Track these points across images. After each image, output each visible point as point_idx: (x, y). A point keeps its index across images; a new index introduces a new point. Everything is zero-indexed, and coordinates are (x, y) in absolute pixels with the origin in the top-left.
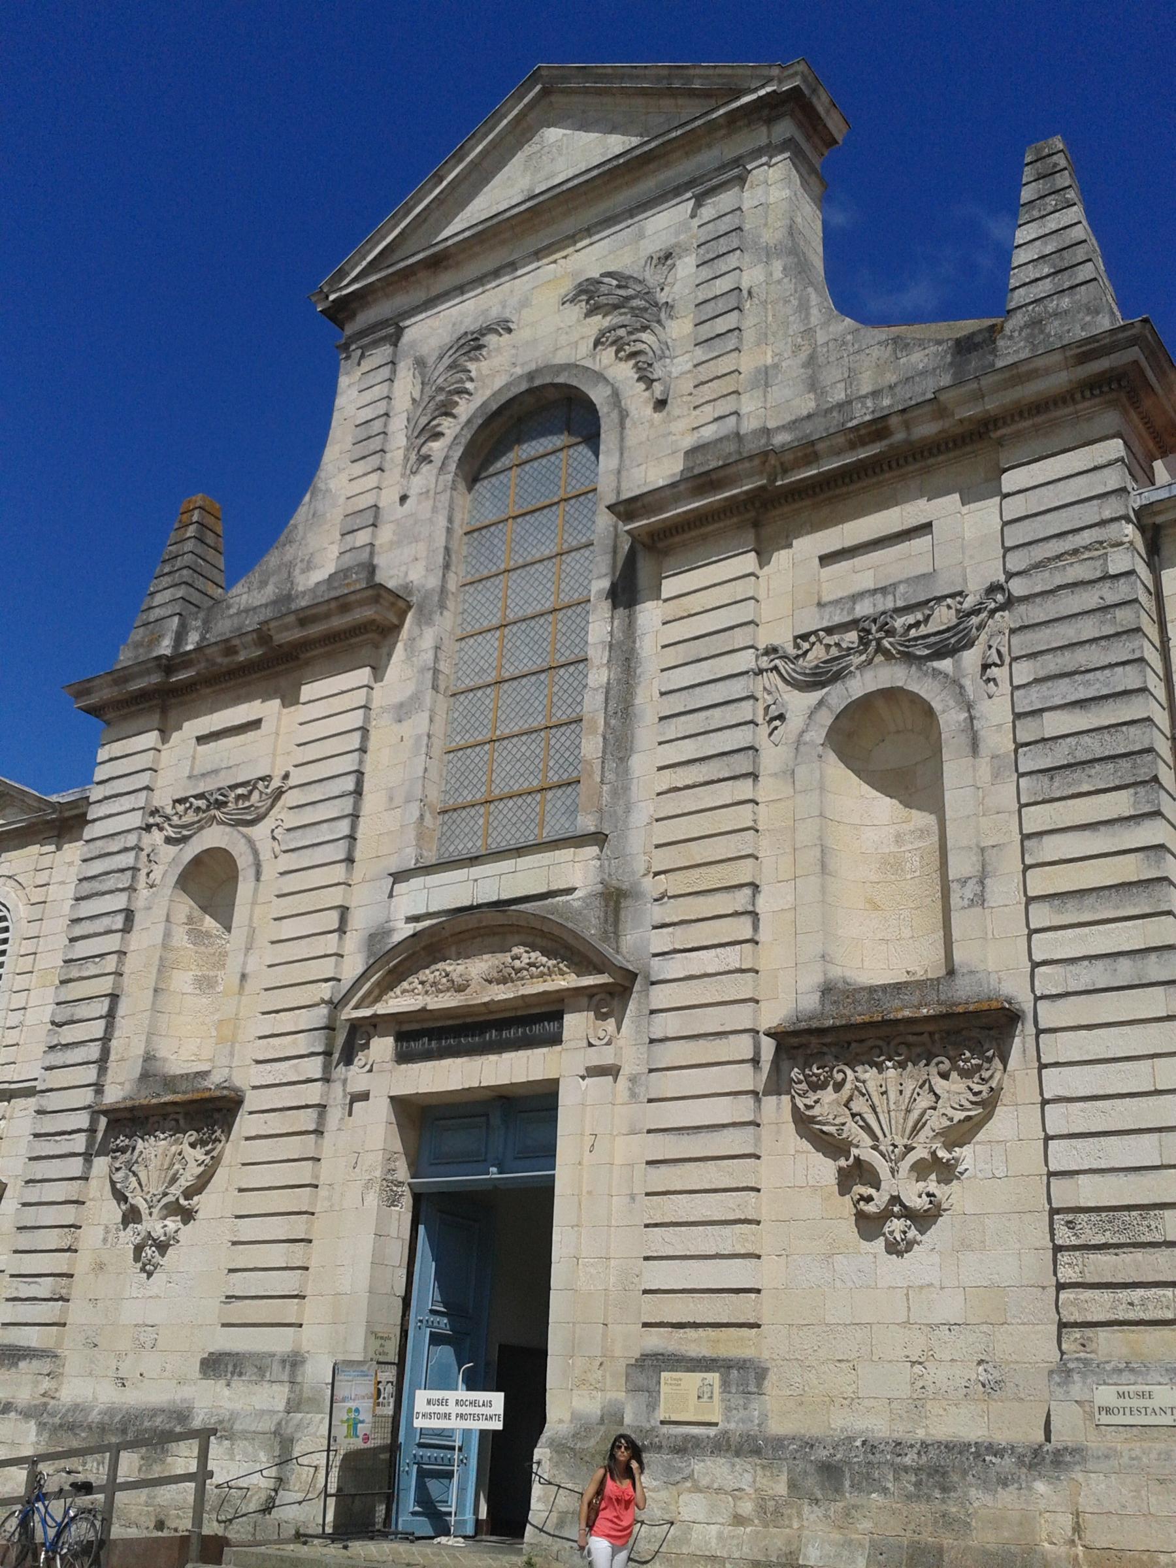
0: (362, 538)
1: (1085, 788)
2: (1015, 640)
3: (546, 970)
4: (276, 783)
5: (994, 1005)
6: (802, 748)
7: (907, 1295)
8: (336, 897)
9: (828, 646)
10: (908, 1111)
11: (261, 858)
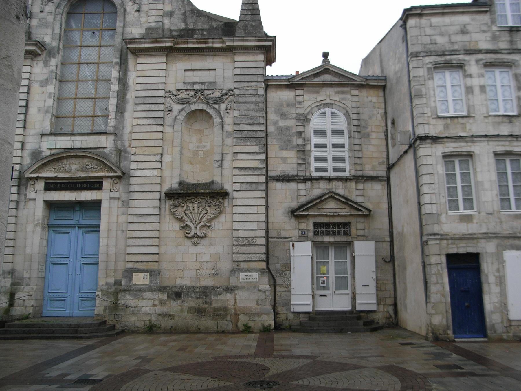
1: (249, 144)
2: (235, 105)
5: (225, 191)
6: (177, 120)
10: (200, 214)
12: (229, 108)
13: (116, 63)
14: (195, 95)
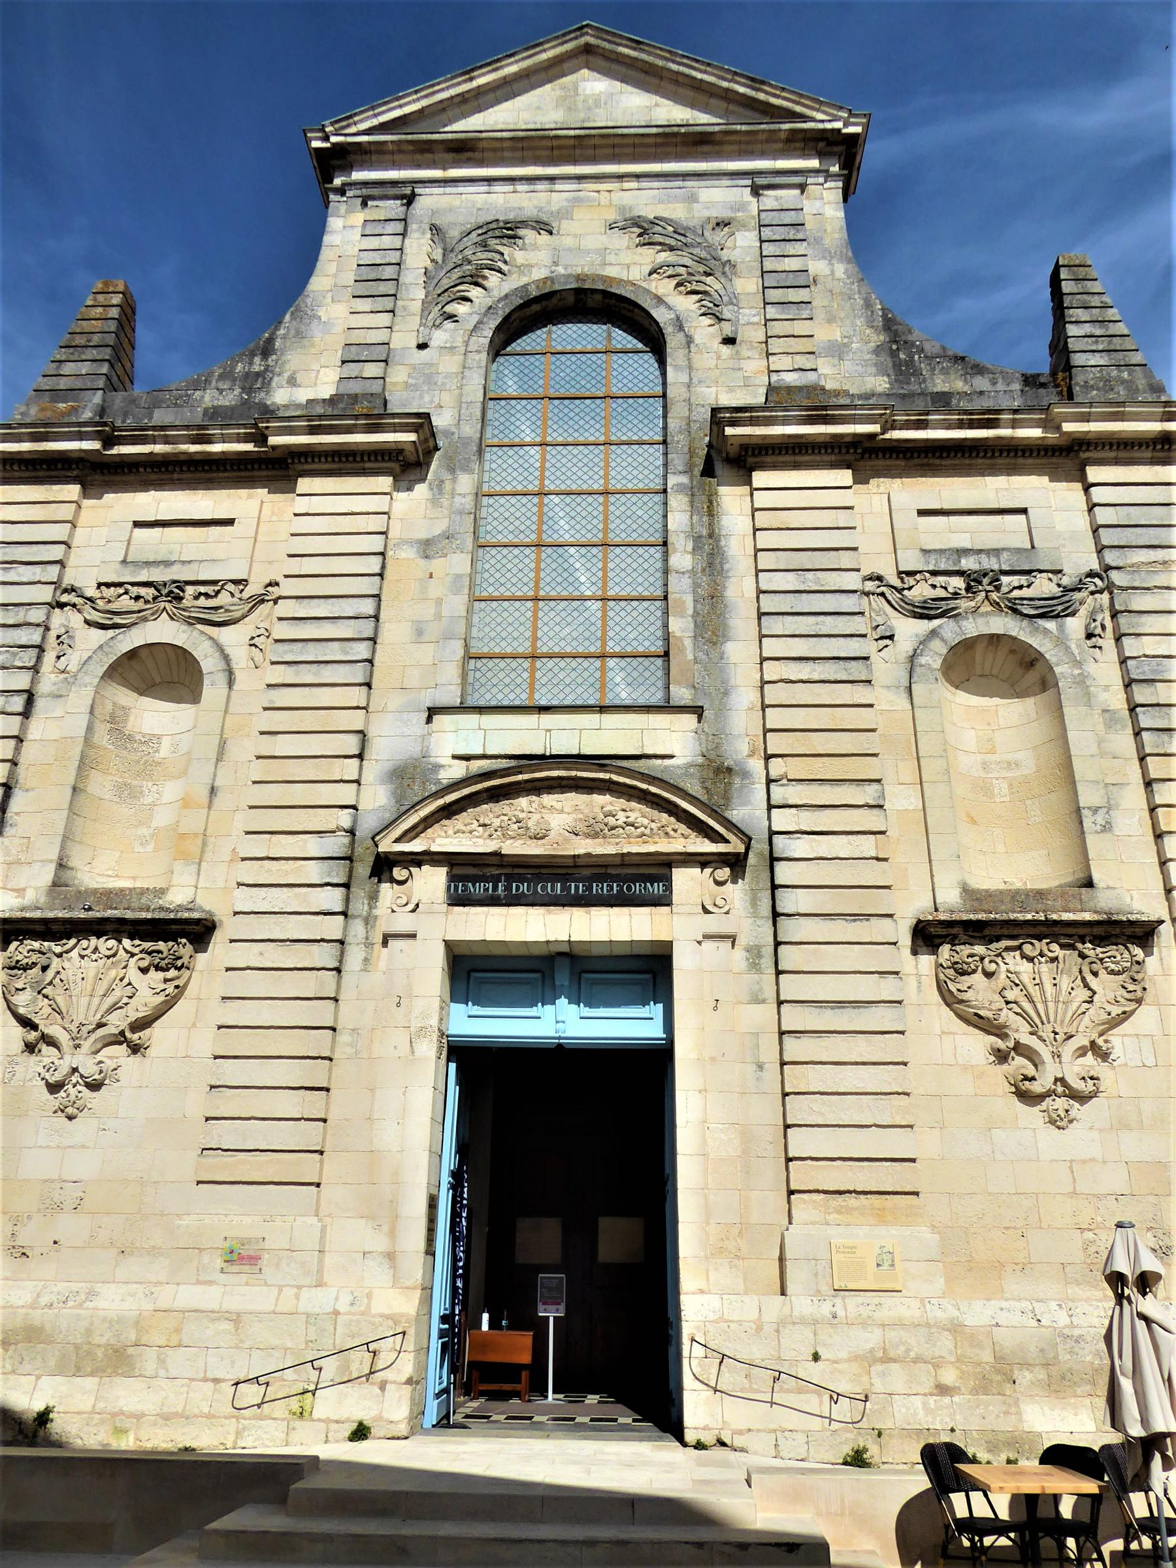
0: (372, 370)
3: (647, 831)
4: (252, 589)
6: (918, 670)
7: (1071, 1168)
8: (355, 720)
9: (934, 586)
11: (234, 665)
12: (1098, 631)
13: (680, 488)
14: (968, 589)
